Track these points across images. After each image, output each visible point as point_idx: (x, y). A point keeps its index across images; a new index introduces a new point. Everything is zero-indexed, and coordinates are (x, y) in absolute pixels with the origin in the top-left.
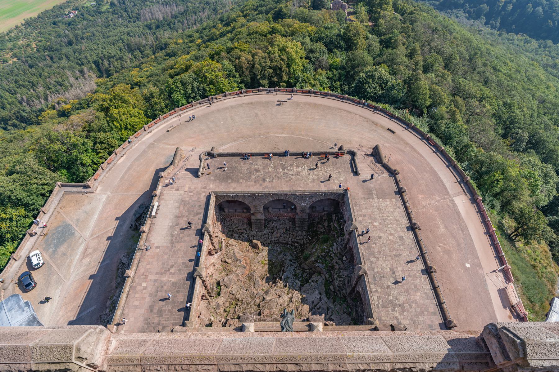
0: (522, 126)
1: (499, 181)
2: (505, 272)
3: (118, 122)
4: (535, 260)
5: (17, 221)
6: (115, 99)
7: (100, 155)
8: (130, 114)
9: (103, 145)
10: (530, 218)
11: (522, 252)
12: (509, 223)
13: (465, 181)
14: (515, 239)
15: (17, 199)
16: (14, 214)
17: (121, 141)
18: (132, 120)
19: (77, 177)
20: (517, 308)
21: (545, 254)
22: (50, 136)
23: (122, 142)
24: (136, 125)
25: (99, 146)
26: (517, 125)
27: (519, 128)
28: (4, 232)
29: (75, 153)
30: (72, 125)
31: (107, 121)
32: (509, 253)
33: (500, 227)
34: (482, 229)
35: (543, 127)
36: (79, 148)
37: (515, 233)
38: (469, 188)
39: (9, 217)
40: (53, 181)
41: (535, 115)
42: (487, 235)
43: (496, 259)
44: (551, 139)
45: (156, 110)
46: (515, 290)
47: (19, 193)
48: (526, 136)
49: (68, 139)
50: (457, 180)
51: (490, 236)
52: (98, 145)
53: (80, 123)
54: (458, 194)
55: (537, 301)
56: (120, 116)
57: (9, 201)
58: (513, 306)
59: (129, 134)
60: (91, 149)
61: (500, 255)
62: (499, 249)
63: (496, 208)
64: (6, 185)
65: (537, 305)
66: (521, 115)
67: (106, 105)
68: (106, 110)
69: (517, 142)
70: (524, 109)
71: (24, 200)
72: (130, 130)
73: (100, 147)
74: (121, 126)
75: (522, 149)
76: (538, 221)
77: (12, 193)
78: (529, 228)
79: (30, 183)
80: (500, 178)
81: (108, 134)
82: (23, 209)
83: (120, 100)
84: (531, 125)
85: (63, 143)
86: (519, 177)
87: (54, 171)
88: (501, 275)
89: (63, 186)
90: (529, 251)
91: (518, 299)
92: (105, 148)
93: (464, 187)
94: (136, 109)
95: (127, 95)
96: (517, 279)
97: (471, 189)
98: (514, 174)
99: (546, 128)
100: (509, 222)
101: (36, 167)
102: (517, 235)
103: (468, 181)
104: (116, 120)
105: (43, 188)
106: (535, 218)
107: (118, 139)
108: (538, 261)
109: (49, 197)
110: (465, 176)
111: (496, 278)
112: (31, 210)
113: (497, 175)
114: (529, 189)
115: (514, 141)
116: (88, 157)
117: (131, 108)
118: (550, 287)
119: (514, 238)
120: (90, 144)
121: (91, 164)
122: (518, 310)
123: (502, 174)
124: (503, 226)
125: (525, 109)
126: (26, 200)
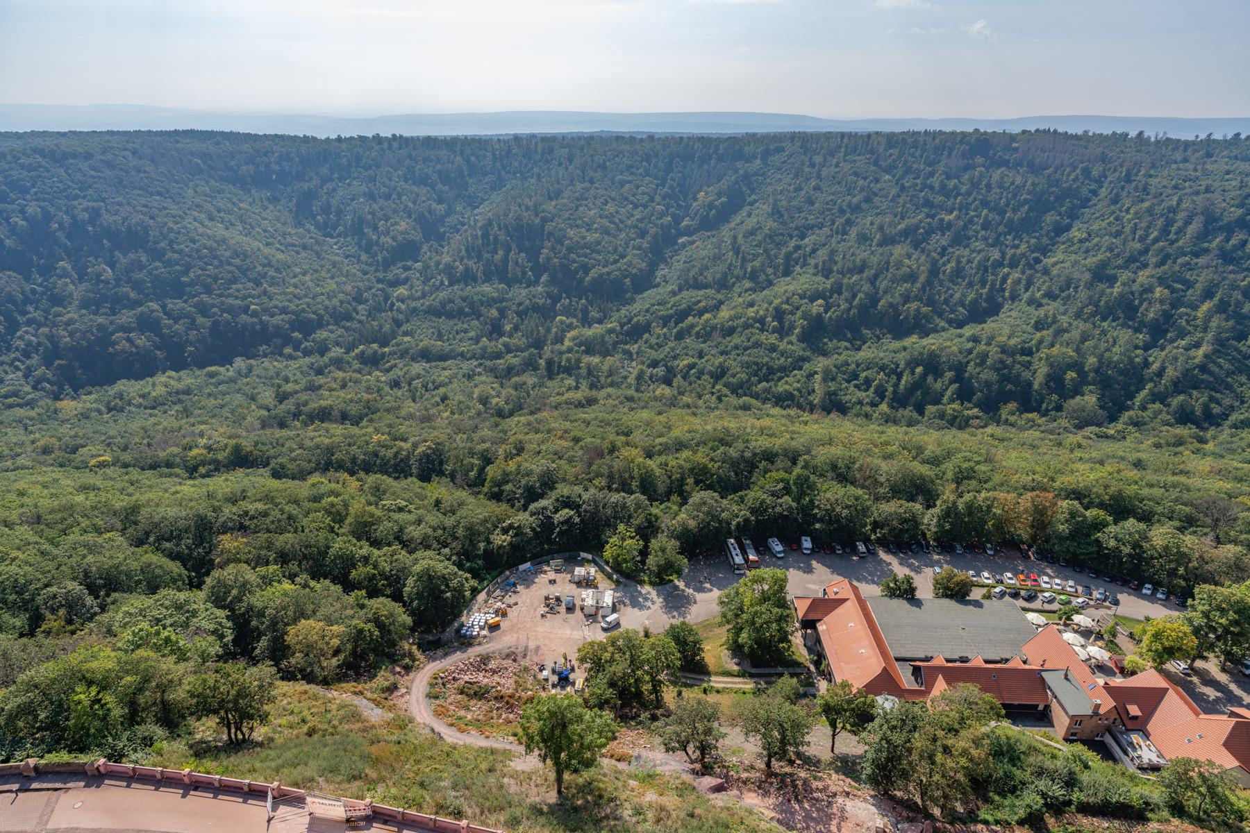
0: (45, 581)
1: (101, 700)
2: (282, 799)
4: (303, 721)
10: (215, 688)
11: (277, 736)
12: (207, 729)
13: (33, 774)
14: (243, 735)
20: (354, 814)
21: (306, 696)
26: (32, 587)
27: (46, 586)
32: (258, 765)
33: (201, 751)
34: (171, 797)
35: (85, 552)
37: (233, 731)
38: (59, 773)
41: (47, 547)
42: (192, 792)
43: (250, 801)
44: (122, 557)
46: (321, 801)
48: (74, 587)
50: (11, 791)
51: (196, 789)
54: (49, 809)
55: (360, 765)
58: (348, 820)
61: (246, 789)
62: (233, 784)
63: (155, 738)
65: (367, 771)
66: (20, 566)
69: (70, 607)
70: (13, 555)
75: (97, 609)
76: (230, 679)
78: (236, 701)
80: (93, 694)
84: (60, 565)
86: (124, 658)
88: (283, 810)
90: (283, 721)
91: (339, 803)
93: (45, 785)
96: (308, 783)
97: (63, 769)
98: (110, 665)
99: (91, 549)
100: (207, 725)
102: (238, 728)
103: (36, 768)
106: (222, 681)
108: (310, 717)
110: (18, 767)
111: (282, 824)
113: (82, 696)
114: (163, 656)
115: (62, 612)
118: (358, 725)
119: (240, 737)
122: (359, 814)
123: (90, 683)
124: (205, 743)
125: (14, 553)
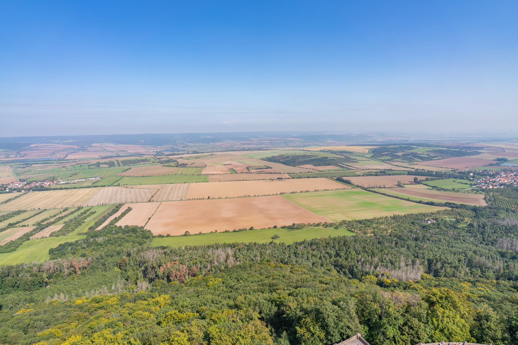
3: (437, 320)
5: (314, 339)
6: (445, 299)
7: (404, 337)
8: (454, 321)
9: (411, 331)
15: (327, 323)
16: (318, 332)
17: (429, 338)
18: (453, 328)
19: (373, 341)
22: (376, 296)
23: (430, 341)
24: (454, 335)
25: (407, 329)
28: (303, 340)
29: (385, 320)
30: (397, 298)
31: (427, 313)
36: (391, 319)
39: (313, 331)
40: (355, 330)
45: (486, 335)
47: (331, 321)
49: (387, 307)
52: (407, 327)
53: (402, 300)
56: (443, 317)
57: (321, 322)
59: (441, 338)
60: (399, 327)
64: (328, 310)
67: (434, 299)
68: (432, 304)
71: (330, 328)
72: (445, 335)
73: (407, 331)
74: (438, 325)
77: (328, 318)
79: (342, 319)
81: (422, 324)
82: (324, 334)
83: (450, 303)
85: (381, 307)
87: (360, 323)
89: (360, 339)
92: (412, 334)
94: (463, 321)
95: (460, 303)
101: (353, 312)
104: (437, 317)
105: (346, 330)
107: (428, 335)
109: (344, 339)
112: (327, 339)
116: (393, 332)
117: (458, 317)
120: (401, 322)
121: (391, 338)
126: (331, 329)
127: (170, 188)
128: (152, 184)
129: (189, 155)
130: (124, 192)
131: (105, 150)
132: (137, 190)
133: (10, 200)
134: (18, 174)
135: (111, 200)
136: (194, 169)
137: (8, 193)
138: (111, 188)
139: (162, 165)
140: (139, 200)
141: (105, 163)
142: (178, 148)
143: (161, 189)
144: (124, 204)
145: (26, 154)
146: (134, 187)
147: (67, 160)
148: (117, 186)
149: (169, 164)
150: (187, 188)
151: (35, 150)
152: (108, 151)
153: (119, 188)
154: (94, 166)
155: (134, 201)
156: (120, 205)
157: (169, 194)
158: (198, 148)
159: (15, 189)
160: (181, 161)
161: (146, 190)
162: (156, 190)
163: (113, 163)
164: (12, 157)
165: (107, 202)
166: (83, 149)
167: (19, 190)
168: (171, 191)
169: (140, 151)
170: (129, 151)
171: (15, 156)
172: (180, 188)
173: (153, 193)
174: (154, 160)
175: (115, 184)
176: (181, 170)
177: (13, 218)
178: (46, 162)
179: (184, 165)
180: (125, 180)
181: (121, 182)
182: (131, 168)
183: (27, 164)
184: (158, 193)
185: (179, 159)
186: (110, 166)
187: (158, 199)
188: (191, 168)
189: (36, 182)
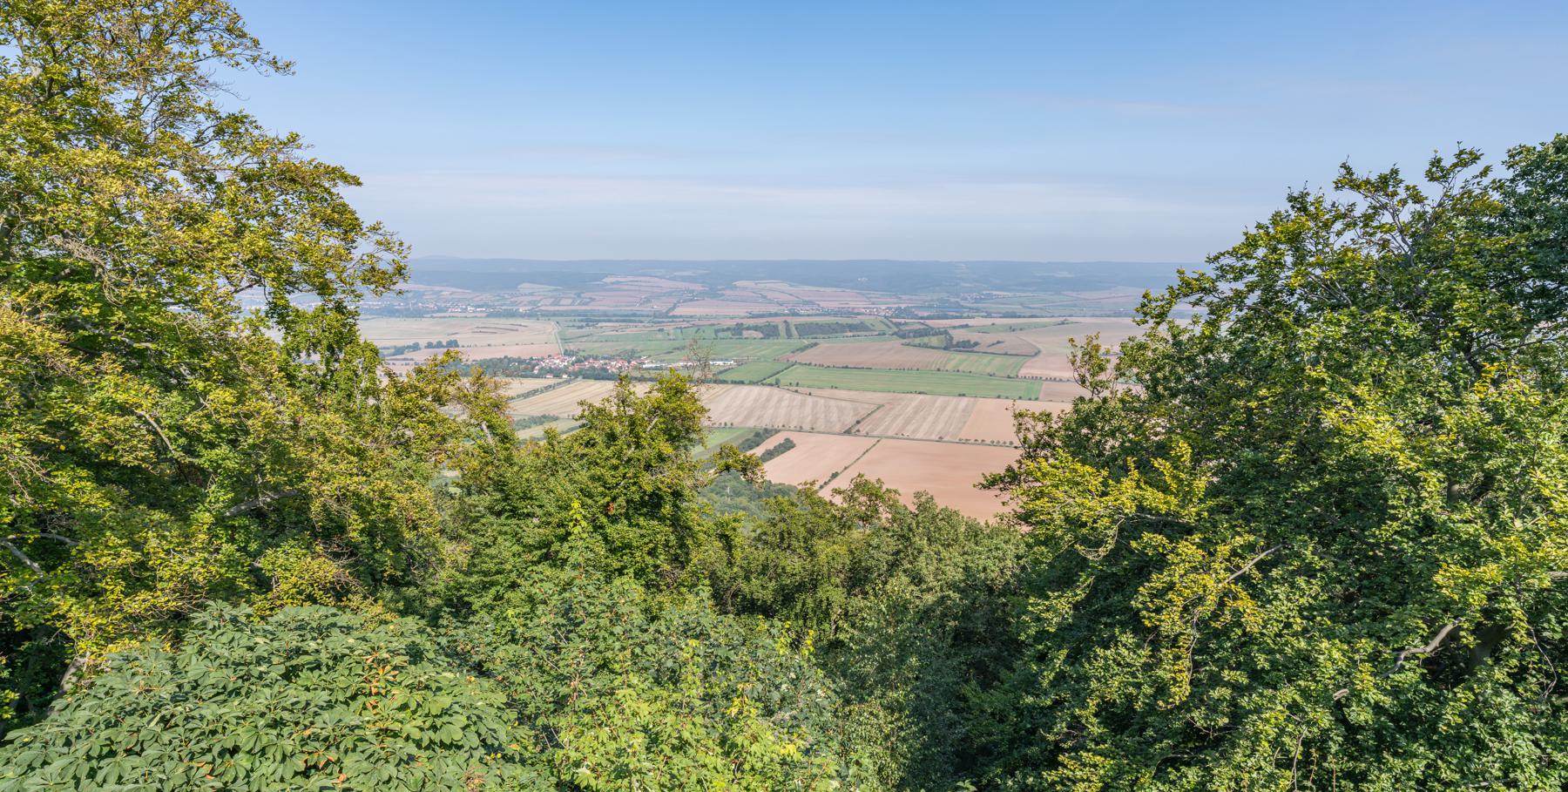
127: (913, 404)
128: (865, 390)
129: (989, 321)
130: (785, 403)
131: (764, 297)
132: (822, 401)
133: (535, 392)
134: (565, 340)
135: (747, 417)
136: (998, 360)
137: (537, 377)
138: (756, 390)
139: (904, 341)
140: (821, 426)
141: (756, 328)
142: (962, 303)
143: (887, 406)
144: (777, 431)
145: (592, 300)
146: (814, 391)
147: (674, 316)
148: (771, 385)
149: (926, 340)
150: (964, 411)
151: (612, 290)
152: (770, 302)
153: (776, 390)
154: (729, 334)
155: (807, 427)
156: (766, 431)
157: (907, 422)
158: (1022, 304)
159: (550, 371)
160: (959, 336)
161: (843, 404)
162: (873, 407)
163: (776, 327)
164: (566, 304)
165: (736, 422)
166: (713, 294)
167: (556, 373)
168: (916, 413)
169: (852, 305)
170: (823, 304)
171: (570, 301)
172: (943, 409)
173: (864, 413)
174: (884, 328)
175: (768, 381)
176: (956, 359)
177: (527, 430)
178: (627, 319)
179: (967, 347)
180: (796, 374)
181: (784, 378)
182: (816, 344)
183: (589, 319)
184: (878, 415)
185: (957, 331)
186: (767, 336)
187: (873, 430)
188: (990, 357)
189: (596, 358)
